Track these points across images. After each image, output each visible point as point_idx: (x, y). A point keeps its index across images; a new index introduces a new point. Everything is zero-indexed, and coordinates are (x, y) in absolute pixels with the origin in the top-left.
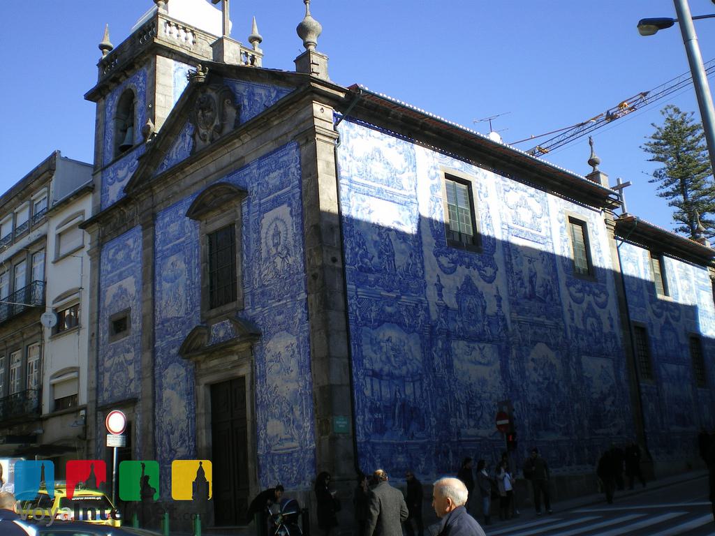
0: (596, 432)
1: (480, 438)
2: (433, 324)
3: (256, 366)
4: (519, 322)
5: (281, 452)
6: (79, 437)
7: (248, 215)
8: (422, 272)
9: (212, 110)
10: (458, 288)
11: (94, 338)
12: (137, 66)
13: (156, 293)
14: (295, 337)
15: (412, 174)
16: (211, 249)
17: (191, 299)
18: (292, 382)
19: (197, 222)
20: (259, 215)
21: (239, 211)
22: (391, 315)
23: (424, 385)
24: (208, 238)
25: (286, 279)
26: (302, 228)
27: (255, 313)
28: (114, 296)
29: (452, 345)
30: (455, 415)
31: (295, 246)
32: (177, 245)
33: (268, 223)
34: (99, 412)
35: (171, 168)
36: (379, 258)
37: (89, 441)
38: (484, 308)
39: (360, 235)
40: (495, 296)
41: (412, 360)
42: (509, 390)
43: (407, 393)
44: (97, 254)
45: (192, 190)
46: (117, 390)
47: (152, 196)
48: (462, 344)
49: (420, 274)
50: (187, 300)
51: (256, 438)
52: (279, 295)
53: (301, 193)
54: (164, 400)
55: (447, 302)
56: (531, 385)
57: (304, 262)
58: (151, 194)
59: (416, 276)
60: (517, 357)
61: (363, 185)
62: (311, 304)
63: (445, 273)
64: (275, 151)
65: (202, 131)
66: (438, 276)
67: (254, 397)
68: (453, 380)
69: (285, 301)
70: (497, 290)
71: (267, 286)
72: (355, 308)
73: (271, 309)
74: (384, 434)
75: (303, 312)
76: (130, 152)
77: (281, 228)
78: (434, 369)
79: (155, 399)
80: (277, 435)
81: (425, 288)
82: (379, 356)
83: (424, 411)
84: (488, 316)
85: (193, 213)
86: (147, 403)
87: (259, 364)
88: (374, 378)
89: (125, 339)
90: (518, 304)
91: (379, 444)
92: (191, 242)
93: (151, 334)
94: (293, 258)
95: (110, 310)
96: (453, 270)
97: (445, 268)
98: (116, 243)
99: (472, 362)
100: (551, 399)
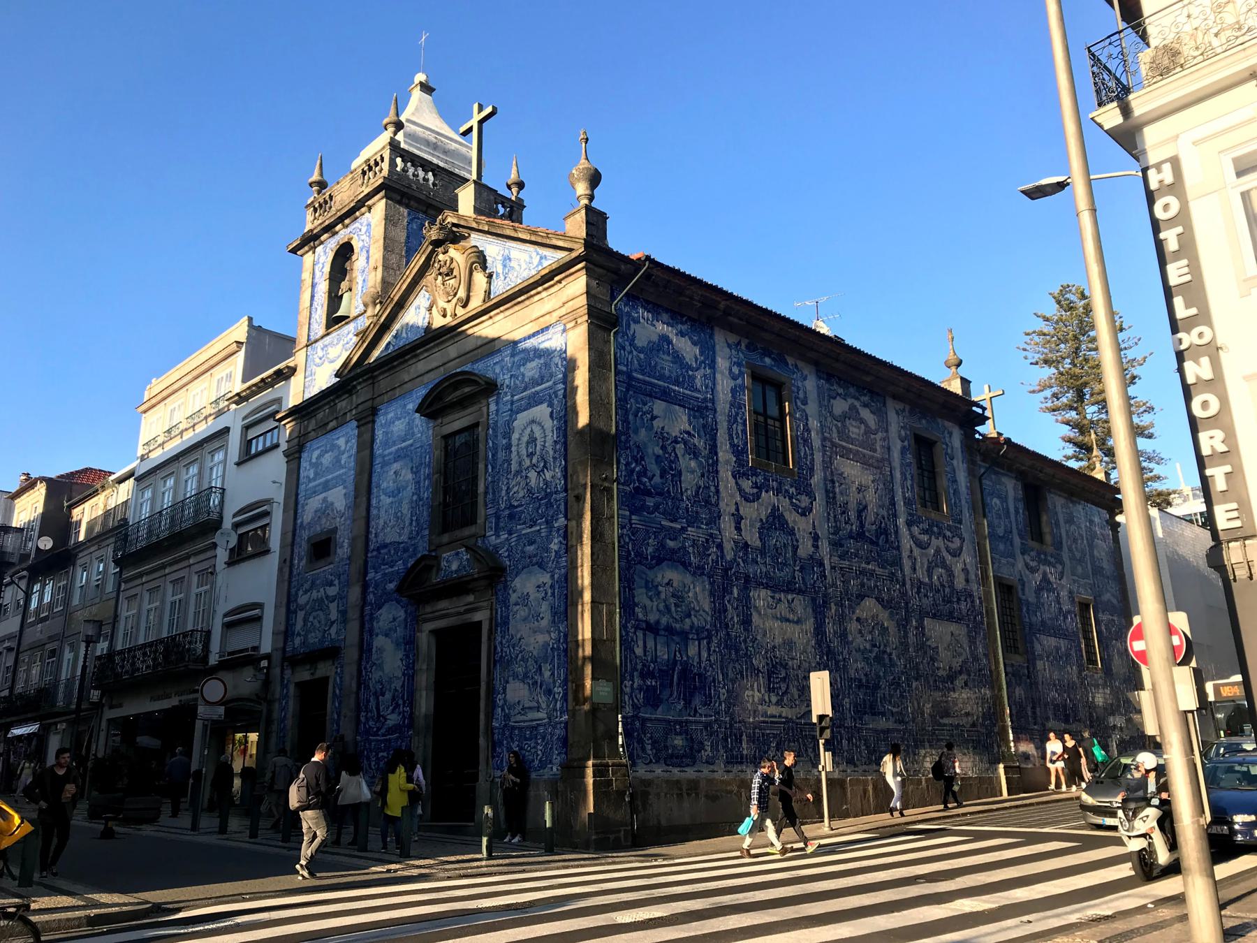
0: (941, 721)
1: (784, 720)
3: (497, 610)
4: (841, 568)
5: (522, 724)
6: (257, 695)
7: (497, 415)
8: (716, 497)
9: (455, 277)
10: (761, 520)
11: (287, 563)
13: (372, 509)
15: (708, 371)
16: (446, 455)
18: (542, 633)
19: (430, 421)
20: (511, 416)
21: (485, 409)
22: (673, 551)
23: (713, 646)
24: (443, 442)
25: (541, 499)
26: (565, 436)
27: (498, 541)
28: (316, 511)
29: (751, 594)
30: (752, 686)
31: (555, 458)
32: (402, 449)
34: (286, 664)
35: (399, 349)
36: (662, 477)
37: (270, 703)
38: (795, 548)
39: (639, 447)
40: (811, 533)
43: (689, 654)
44: (294, 455)
45: (426, 378)
46: (313, 634)
47: (373, 383)
49: (713, 501)
51: (492, 705)
53: (565, 389)
54: (374, 650)
55: (748, 539)
56: (854, 652)
57: (565, 477)
58: (371, 381)
59: (707, 502)
61: (645, 382)
62: (572, 533)
63: (747, 500)
65: (441, 303)
66: (736, 504)
67: (492, 651)
68: (751, 641)
69: (538, 528)
70: (814, 526)
71: (516, 507)
72: (627, 540)
74: (658, 707)
76: (347, 323)
77: (538, 433)
79: (365, 649)
80: (519, 702)
81: (719, 519)
84: (800, 559)
86: (351, 654)
87: (501, 608)
89: (326, 568)
90: (842, 546)
91: (650, 720)
92: (421, 447)
94: (551, 473)
95: (309, 530)
96: (757, 497)
97: (746, 493)
98: (323, 441)
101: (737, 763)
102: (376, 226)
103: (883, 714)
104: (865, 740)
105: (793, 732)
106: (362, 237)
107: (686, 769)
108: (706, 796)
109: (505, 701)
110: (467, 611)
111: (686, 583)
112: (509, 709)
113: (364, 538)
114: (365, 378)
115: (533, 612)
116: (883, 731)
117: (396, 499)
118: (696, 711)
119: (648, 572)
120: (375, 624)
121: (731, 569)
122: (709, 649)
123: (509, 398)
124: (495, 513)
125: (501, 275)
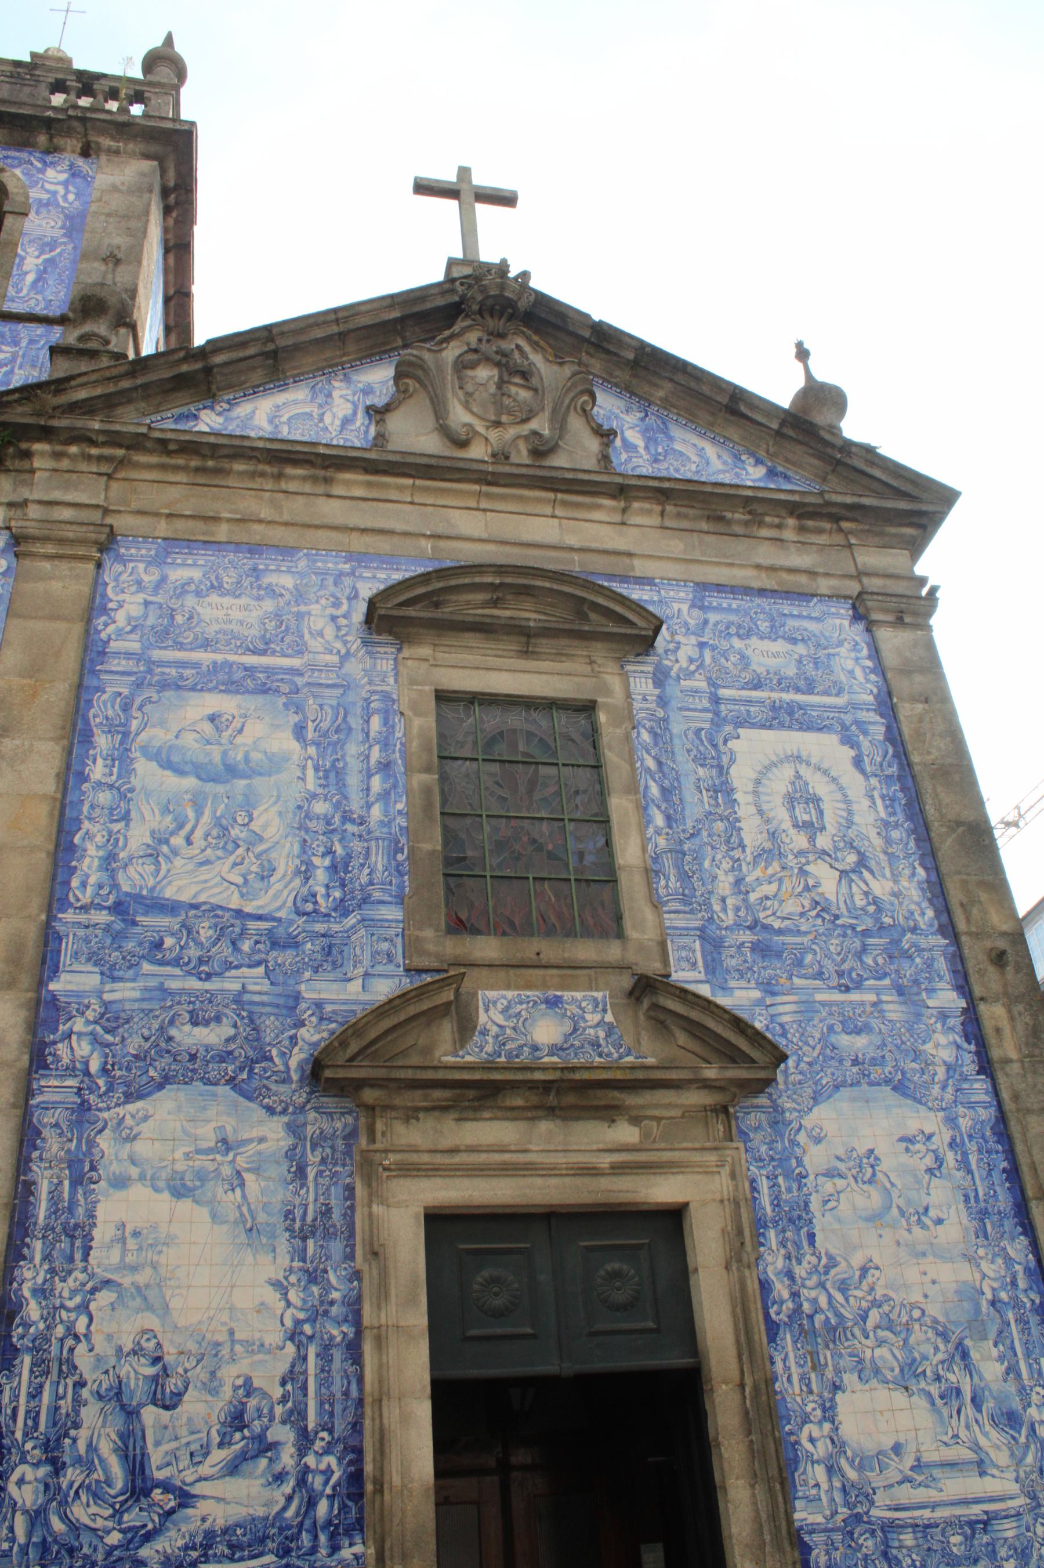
3: (753, 1181)
12: (42, 139)
14: (941, 1114)
17: (333, 868)
21: (615, 683)
25: (866, 933)
32: (249, 670)
33: (767, 762)
50: (309, 864)
52: (840, 974)
54: (101, 1234)
62: (998, 1030)
64: (762, 592)
69: (872, 997)
73: (808, 1009)
75: (958, 1047)
77: (819, 786)
80: (897, 1449)
85: (401, 605)
92: (347, 688)
93: (32, 933)
94: (889, 885)
102: (115, 189)
106: (47, 186)
109: (838, 1444)
110: (618, 1169)
112: (860, 1468)
113: (41, 859)
114: (94, 451)
115: (896, 1201)
117: (220, 789)
120: (105, 1142)
123: (703, 685)
124: (702, 929)
125: (642, 451)
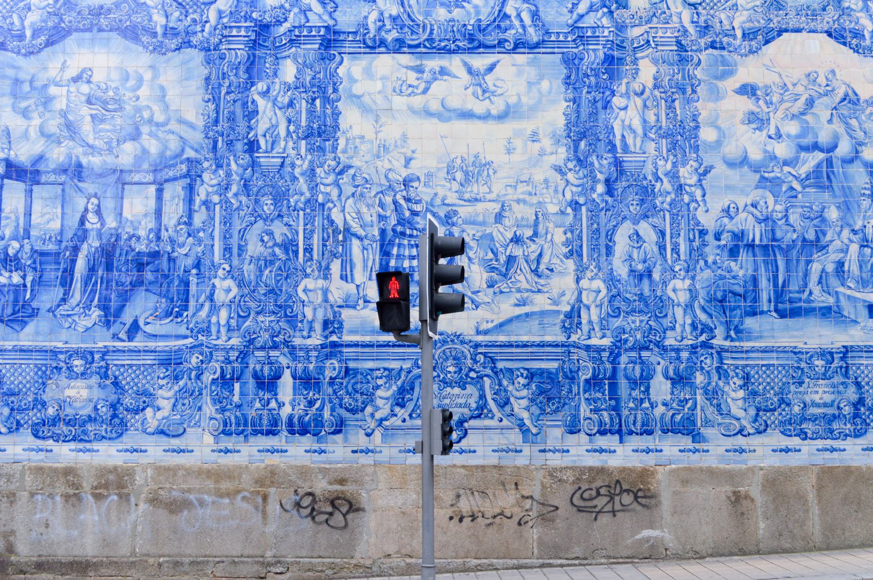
2: (267, 18)
29: (341, 71)
41: (158, 125)
42: (600, 188)
43: (126, 214)
48: (384, 63)
56: (720, 169)
60: (656, 87)
78: (252, 146)
82: (36, 121)
83: (190, 261)
88: (6, 181)
99: (428, 113)
100: (833, 214)
101: (256, 433)
103: (826, 312)
104: (747, 378)
105: (456, 365)
107: (96, 446)
108: (154, 500)
111: (130, 70)
116: (827, 355)
118: (134, 329)
119: (20, 61)
121: (279, 23)
122: (190, 201)
